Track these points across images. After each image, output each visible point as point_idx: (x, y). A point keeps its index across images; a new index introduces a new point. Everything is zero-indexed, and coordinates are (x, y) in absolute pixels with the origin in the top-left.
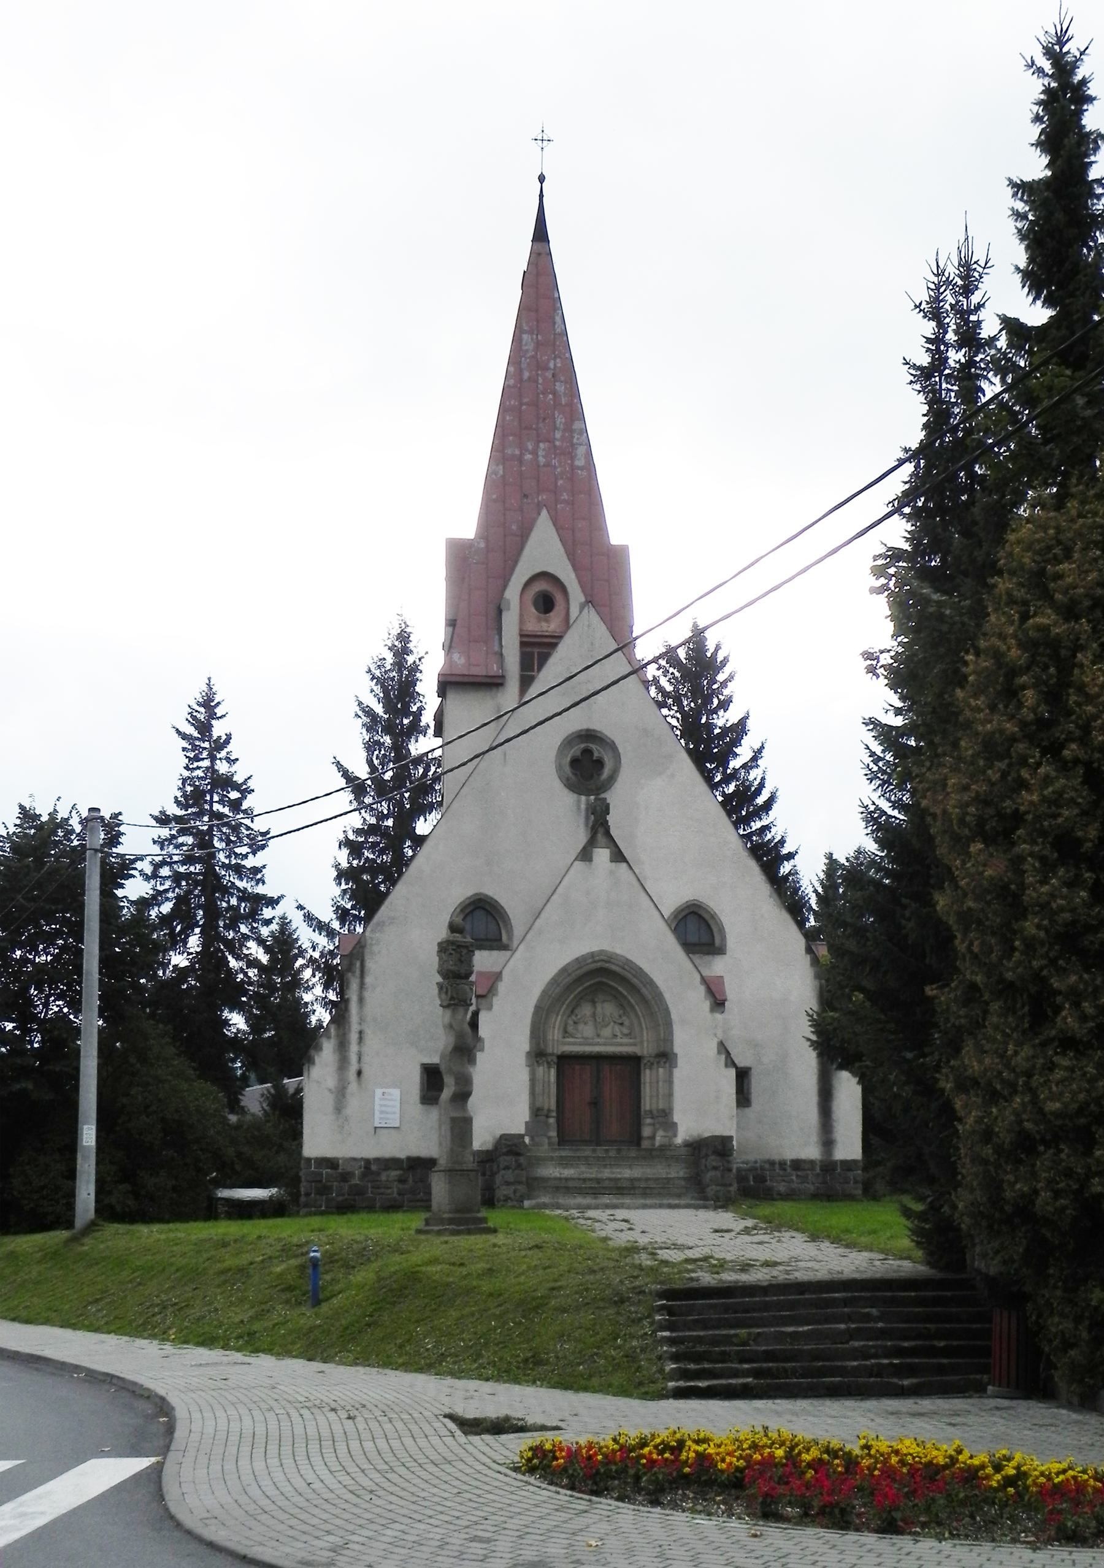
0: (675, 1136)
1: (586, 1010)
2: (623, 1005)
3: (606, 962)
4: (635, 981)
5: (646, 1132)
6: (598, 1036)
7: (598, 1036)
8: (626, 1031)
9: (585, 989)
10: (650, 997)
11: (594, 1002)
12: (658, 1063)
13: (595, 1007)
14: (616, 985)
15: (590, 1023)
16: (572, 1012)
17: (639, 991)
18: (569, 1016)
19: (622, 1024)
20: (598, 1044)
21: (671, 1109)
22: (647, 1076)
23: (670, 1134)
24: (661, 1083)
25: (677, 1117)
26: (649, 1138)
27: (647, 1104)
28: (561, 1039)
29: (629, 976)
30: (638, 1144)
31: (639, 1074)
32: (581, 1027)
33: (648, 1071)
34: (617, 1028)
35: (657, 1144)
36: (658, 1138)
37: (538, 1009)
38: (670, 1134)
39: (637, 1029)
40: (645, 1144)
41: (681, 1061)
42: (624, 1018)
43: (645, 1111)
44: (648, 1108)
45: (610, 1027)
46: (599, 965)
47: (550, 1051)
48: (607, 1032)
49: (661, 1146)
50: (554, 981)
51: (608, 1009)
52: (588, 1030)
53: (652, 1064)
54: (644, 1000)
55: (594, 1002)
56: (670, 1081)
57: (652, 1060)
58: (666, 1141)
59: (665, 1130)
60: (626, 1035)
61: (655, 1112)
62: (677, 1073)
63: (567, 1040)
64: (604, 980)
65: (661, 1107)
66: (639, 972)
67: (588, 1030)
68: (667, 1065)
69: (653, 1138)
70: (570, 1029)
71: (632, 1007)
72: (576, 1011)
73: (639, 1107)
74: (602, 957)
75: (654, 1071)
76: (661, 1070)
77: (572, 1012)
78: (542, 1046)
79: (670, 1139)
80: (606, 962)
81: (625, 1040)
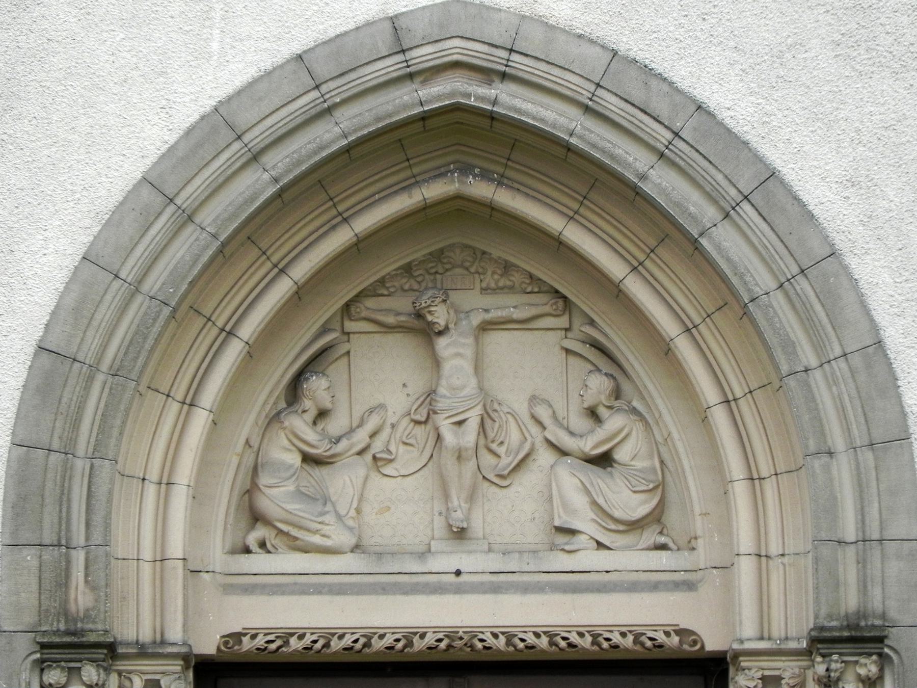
1: (379, 379)
2: (565, 292)
3: (487, 74)
4: (662, 183)
6: (460, 534)
7: (460, 534)
8: (636, 506)
9: (360, 248)
10: (763, 280)
11: (424, 331)
13: (437, 362)
14: (552, 221)
15: (407, 459)
16: (294, 390)
17: (692, 248)
18: (275, 418)
19: (604, 460)
20: (457, 583)
28: (216, 555)
29: (632, 159)
32: (343, 482)
34: (570, 481)
37: (55, 366)
39: (695, 486)
42: (614, 422)
45: (528, 483)
46: (437, 93)
47: (133, 625)
48: (512, 513)
50: (160, 194)
51: (521, 370)
52: (397, 505)
54: (730, 301)
55: (424, 331)
60: (635, 526)
63: (258, 562)
64: (481, 189)
66: (694, 133)
67: (397, 505)
70: (277, 497)
71: (665, 351)
72: (317, 387)
74: (455, 49)
77: (294, 390)
78: (81, 598)
80: (487, 74)
81: (632, 558)
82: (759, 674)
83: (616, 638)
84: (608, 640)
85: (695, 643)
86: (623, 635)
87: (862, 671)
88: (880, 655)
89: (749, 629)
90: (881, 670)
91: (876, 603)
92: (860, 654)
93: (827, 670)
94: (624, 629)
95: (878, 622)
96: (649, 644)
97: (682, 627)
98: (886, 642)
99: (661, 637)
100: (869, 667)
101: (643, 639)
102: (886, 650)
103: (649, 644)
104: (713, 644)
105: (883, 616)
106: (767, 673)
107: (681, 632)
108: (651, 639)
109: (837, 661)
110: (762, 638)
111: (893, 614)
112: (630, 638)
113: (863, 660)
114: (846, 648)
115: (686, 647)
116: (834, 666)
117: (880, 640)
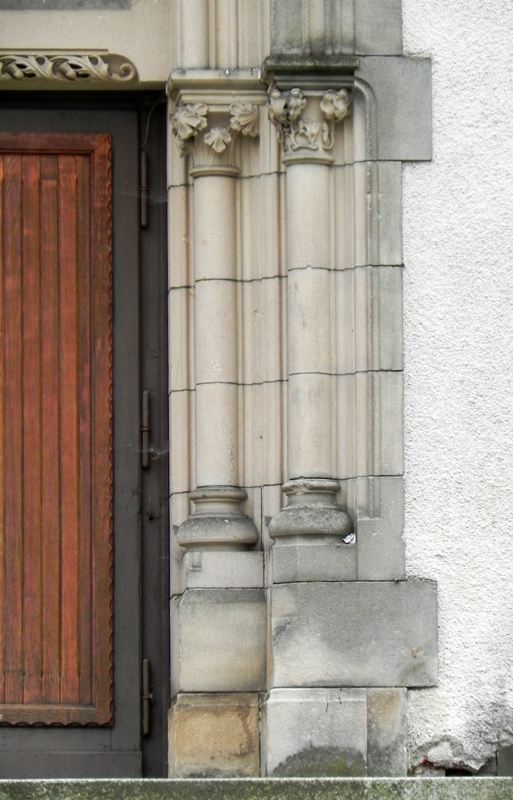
0: (418, 681)
5: (202, 649)
12: (286, 124)
21: (387, 478)
22: (201, 221)
23: (379, 667)
24: (305, 284)
25: (429, 538)
26: (214, 696)
27: (201, 452)
30: (151, 753)
31: (152, 222)
33: (210, 193)
35: (279, 746)
36: (282, 702)
38: (379, 667)
40: (194, 743)
41: (456, 114)
43: (196, 497)
44: (213, 473)
49: (309, 759)
53: (246, 140)
56: (382, 272)
57: (239, 106)
58: (348, 725)
59: (343, 639)
61: (268, 506)
62: (428, 203)
65: (307, 464)
68: (357, 141)
69: (250, 695)
73: (155, 467)
75: (259, 194)
76: (306, 182)
79: (378, 698)
82: (204, 111)
83: (32, 65)
84: (22, 66)
85: (127, 71)
86: (40, 61)
87: (328, 109)
88: (349, 90)
89: (191, 56)
90: (350, 108)
91: (346, 29)
92: (325, 89)
93: (286, 107)
94: (41, 54)
95: (347, 50)
96: (71, 72)
97: (111, 52)
98: (357, 74)
99: (86, 65)
100: (335, 104)
101: (64, 66)
102: (357, 84)
103: (71, 72)
104: (149, 72)
105: (354, 43)
106: (213, 109)
107: (110, 59)
108: (74, 66)
109: (297, 97)
110: (207, 68)
111: (365, 41)
112: (49, 65)
113: (328, 96)
114: (309, 81)
115: (116, 77)
116: (293, 102)
117: (350, 72)
